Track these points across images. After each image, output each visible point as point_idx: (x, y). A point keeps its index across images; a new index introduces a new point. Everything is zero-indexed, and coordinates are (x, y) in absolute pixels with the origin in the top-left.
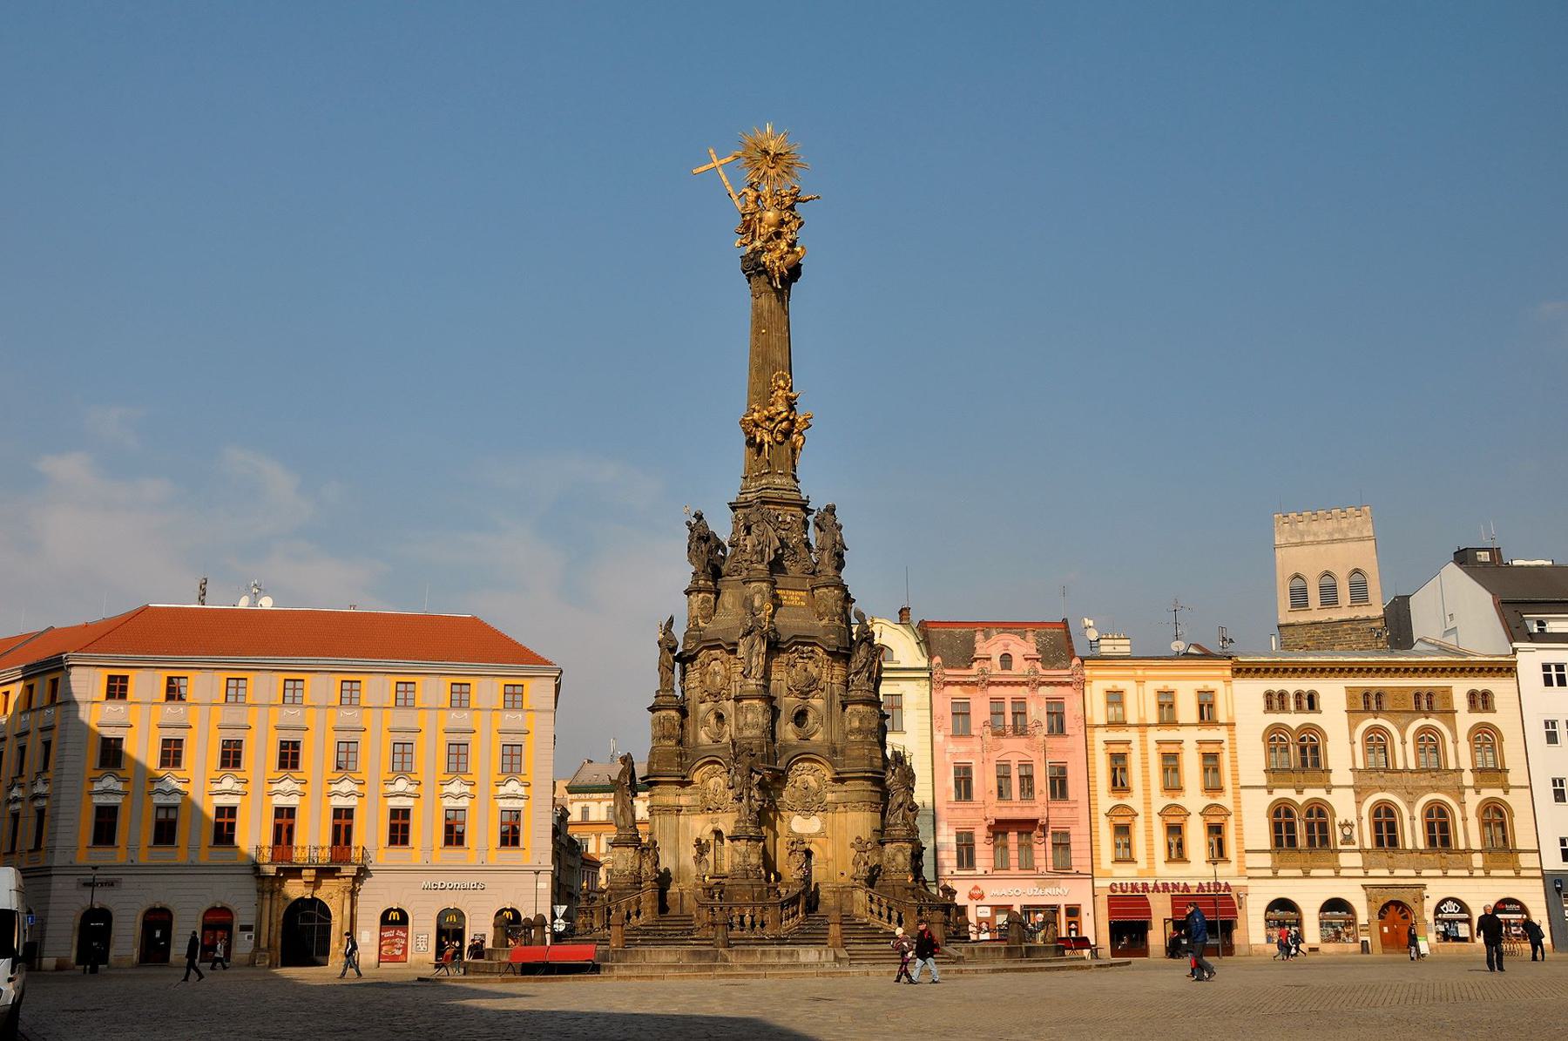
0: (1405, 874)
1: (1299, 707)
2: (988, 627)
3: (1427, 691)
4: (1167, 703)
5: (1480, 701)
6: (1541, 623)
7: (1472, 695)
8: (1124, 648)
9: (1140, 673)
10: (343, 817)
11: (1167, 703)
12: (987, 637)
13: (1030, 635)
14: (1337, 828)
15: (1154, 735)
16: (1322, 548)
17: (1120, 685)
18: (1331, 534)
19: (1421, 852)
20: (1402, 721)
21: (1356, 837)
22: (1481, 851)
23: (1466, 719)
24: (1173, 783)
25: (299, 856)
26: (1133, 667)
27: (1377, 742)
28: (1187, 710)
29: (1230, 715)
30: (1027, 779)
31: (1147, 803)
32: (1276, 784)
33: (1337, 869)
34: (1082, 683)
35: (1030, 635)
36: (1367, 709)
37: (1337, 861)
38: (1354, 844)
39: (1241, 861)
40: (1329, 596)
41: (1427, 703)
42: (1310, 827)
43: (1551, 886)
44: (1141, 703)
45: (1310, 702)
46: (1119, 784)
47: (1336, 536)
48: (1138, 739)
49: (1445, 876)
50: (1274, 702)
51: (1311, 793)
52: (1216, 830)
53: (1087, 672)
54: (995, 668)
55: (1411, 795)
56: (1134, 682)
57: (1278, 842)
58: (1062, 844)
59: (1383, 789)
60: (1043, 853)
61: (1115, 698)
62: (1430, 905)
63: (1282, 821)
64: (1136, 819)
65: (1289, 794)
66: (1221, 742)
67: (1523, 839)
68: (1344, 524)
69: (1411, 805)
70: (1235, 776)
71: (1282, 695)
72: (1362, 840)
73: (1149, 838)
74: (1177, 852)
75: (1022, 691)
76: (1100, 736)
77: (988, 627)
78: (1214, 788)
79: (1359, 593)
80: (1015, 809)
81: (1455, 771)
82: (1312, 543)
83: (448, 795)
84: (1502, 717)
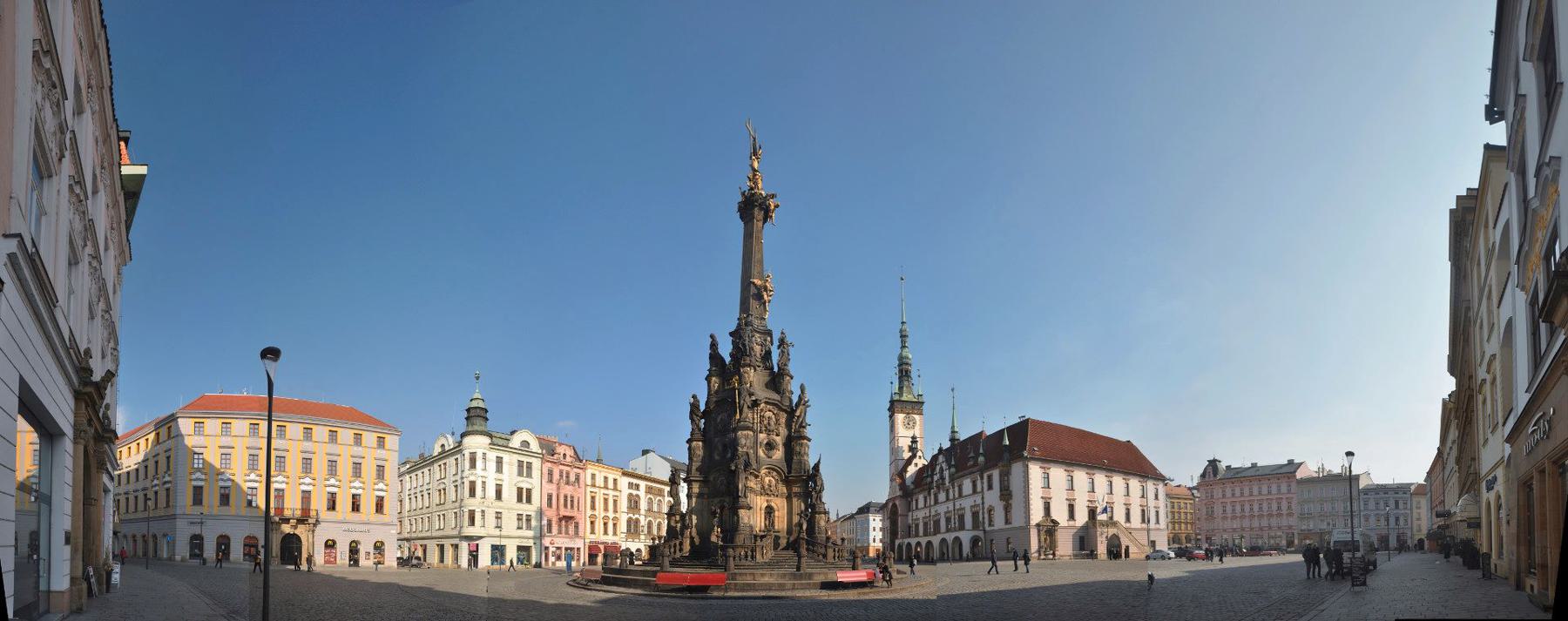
10: (306, 496)
15: (603, 491)
24: (606, 509)
25: (287, 513)
27: (650, 502)
44: (600, 481)
45: (637, 487)
46: (593, 508)
51: (637, 516)
52: (615, 525)
55: (655, 518)
61: (593, 476)
65: (631, 515)
76: (589, 489)
78: (615, 511)
83: (354, 487)
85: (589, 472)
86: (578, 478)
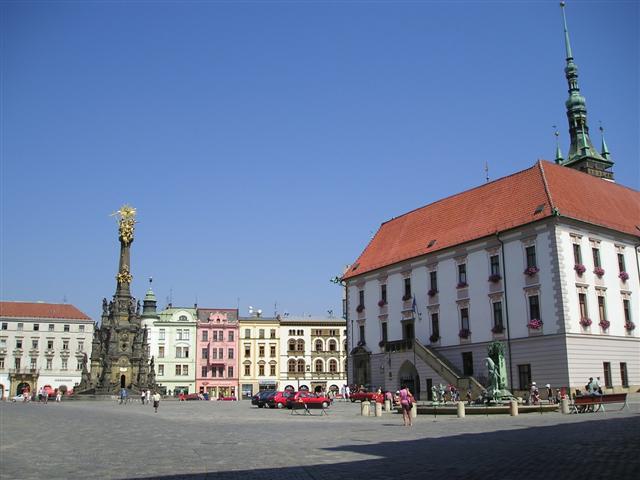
0: (323, 378)
2: (214, 311)
4: (262, 332)
11: (262, 332)
28: (267, 335)
30: (221, 353)
41: (334, 333)
44: (255, 332)
45: (301, 333)
50: (292, 332)
51: (299, 357)
52: (273, 367)
55: (325, 358)
58: (231, 369)
61: (248, 331)
65: (293, 357)
73: (255, 369)
74: (262, 373)
77: (214, 311)
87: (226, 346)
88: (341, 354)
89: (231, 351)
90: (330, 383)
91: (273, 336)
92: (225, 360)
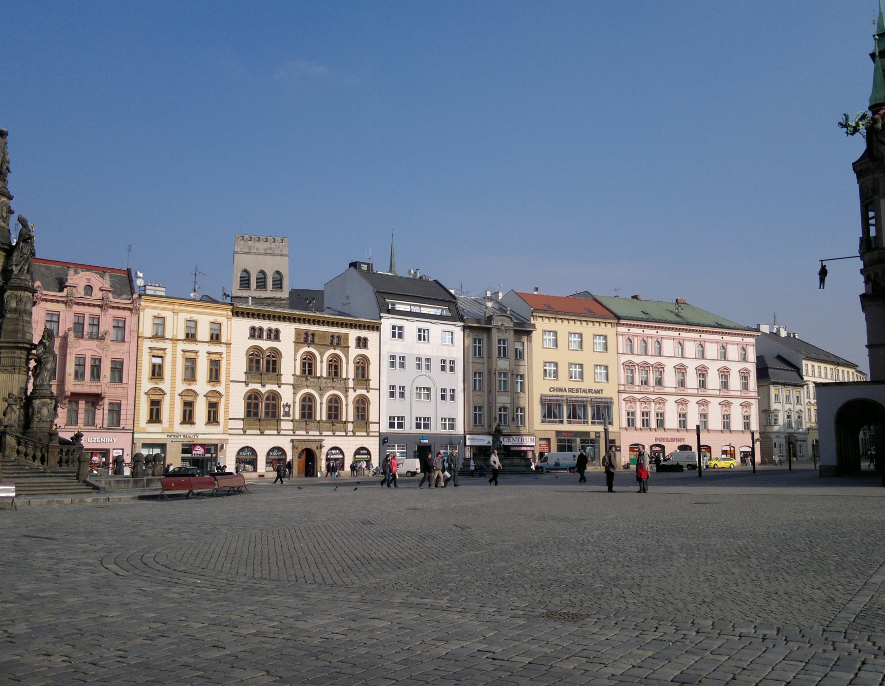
1: (269, 338)
3: (337, 335)
5: (362, 343)
6: (393, 304)
7: (359, 339)
8: (161, 292)
9: (176, 307)
12: (76, 272)
13: (107, 276)
14: (282, 407)
15: (182, 346)
16: (260, 257)
17: (163, 313)
18: (266, 250)
19: (324, 422)
20: (322, 350)
21: (291, 413)
22: (352, 422)
23: (354, 352)
26: (173, 304)
28: (203, 333)
29: (229, 338)
31: (173, 387)
32: (251, 380)
33: (279, 431)
34: (138, 310)
35: (107, 276)
36: (306, 341)
37: (280, 426)
38: (289, 416)
39: (226, 424)
40: (262, 283)
41: (338, 341)
42: (267, 406)
43: (382, 441)
44: (176, 326)
45: (275, 335)
47: (269, 251)
48: (171, 348)
49: (334, 435)
50: (255, 333)
52: (213, 408)
53: (142, 303)
54: (81, 292)
55: (321, 391)
56: (171, 312)
57: (248, 414)
58: (116, 410)
59: (307, 387)
60: (102, 415)
61: (160, 322)
62: (325, 450)
63: (252, 400)
64: (165, 397)
65: (258, 387)
66: (221, 354)
67: (373, 416)
68: (273, 245)
69: (321, 396)
70: (228, 375)
71: (261, 329)
72: (294, 415)
73: (172, 409)
74: (188, 418)
75: (97, 311)
79: (278, 283)
80: (87, 386)
81: (345, 379)
82: (255, 254)
84: (371, 353)
85: (148, 314)
86: (120, 327)
87: (109, 352)
88: (351, 384)
89: (118, 369)
90: (329, 442)
91: (215, 338)
92: (105, 386)
